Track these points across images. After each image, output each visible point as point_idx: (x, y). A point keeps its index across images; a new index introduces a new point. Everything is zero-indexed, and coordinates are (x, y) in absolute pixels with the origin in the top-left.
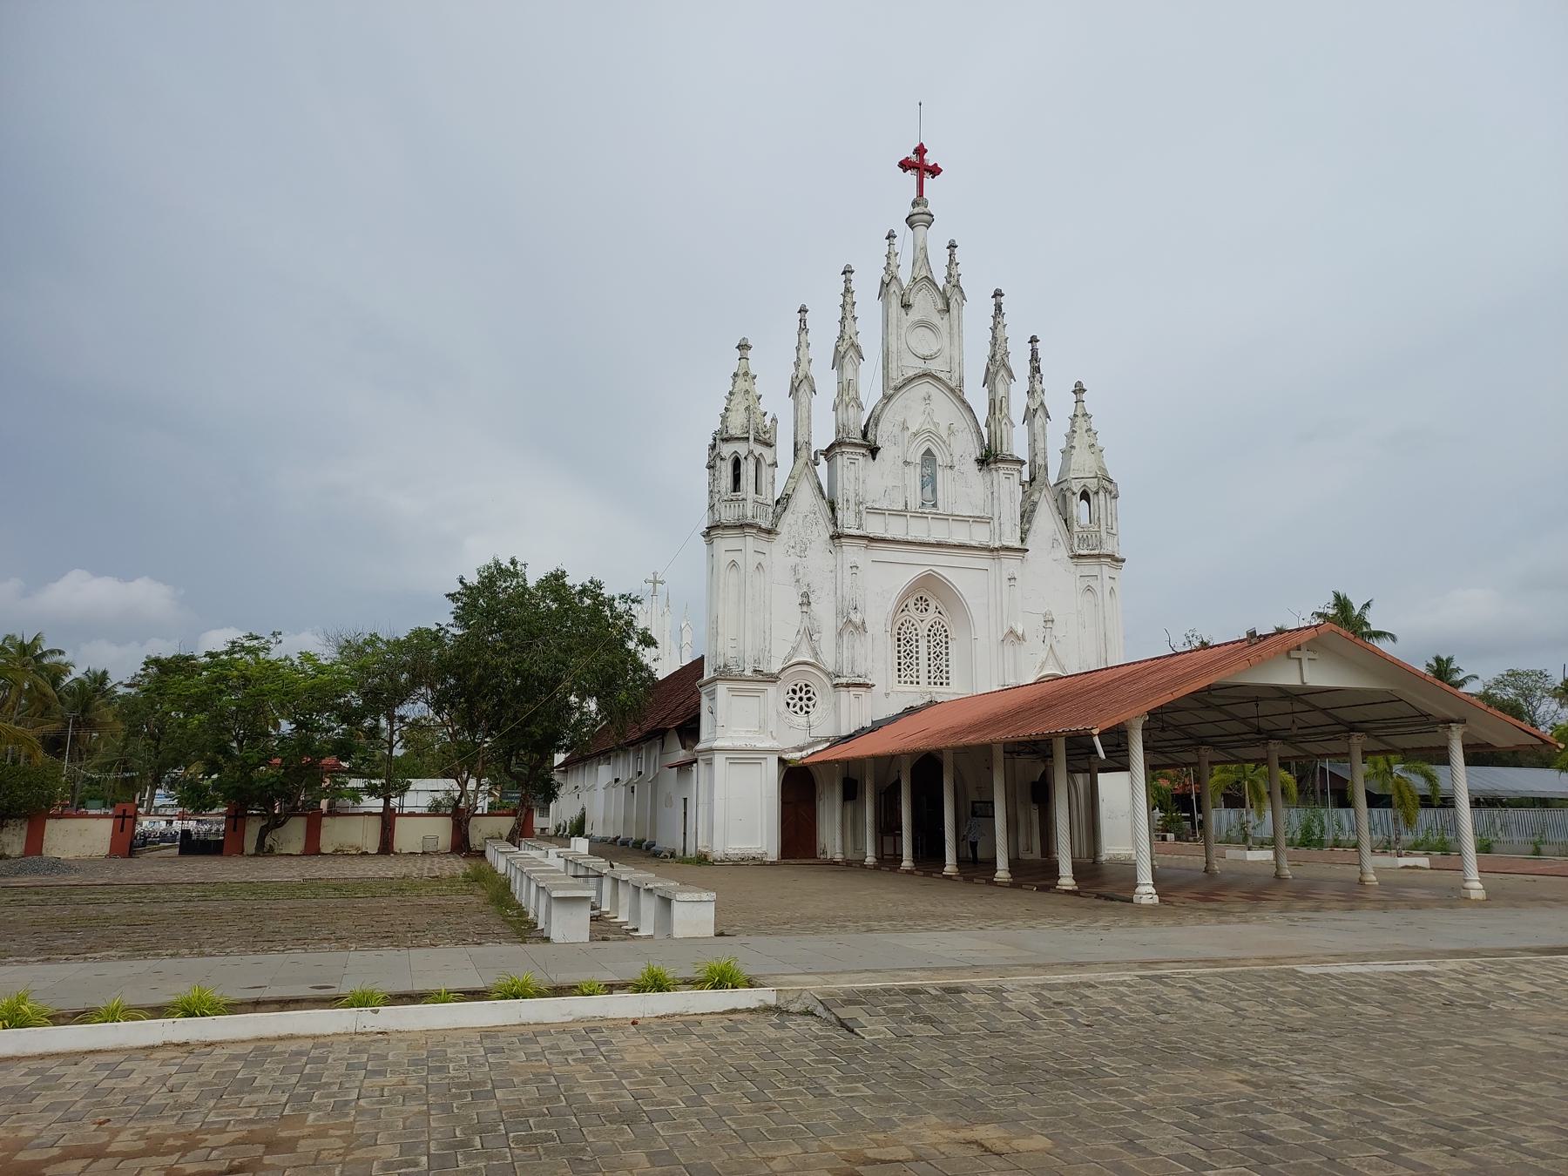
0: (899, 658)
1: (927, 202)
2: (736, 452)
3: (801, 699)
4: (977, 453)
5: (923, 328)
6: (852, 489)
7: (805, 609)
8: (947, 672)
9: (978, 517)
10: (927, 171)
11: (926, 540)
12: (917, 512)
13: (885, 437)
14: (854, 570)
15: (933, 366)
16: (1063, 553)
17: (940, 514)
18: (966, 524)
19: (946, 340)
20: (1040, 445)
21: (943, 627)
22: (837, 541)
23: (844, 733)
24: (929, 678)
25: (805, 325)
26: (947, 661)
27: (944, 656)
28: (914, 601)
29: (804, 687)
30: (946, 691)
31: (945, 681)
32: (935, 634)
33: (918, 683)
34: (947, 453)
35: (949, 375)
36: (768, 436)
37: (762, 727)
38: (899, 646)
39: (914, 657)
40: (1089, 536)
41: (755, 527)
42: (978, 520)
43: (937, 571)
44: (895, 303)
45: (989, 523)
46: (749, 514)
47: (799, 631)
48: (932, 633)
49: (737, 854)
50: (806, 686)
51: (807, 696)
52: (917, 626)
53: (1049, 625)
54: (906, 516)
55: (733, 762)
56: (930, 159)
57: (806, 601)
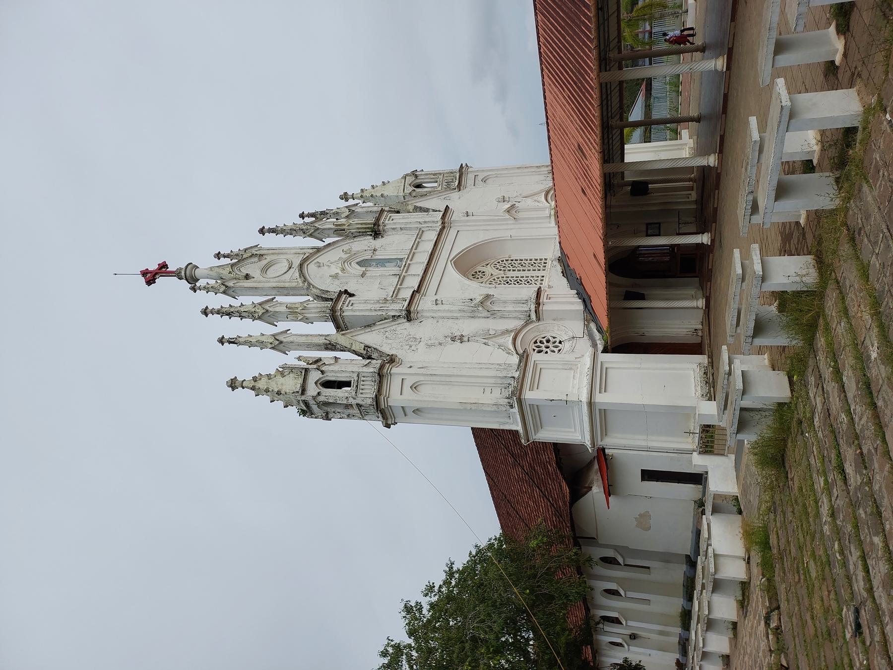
3: (547, 347)
7: (465, 339)
19: (282, 256)
22: (412, 315)
23: (581, 307)
25: (233, 338)
27: (522, 262)
29: (536, 345)
37: (569, 366)
40: (446, 181)
43: (452, 257)
45: (423, 231)
47: (485, 344)
50: (536, 342)
51: (545, 342)
55: (604, 389)
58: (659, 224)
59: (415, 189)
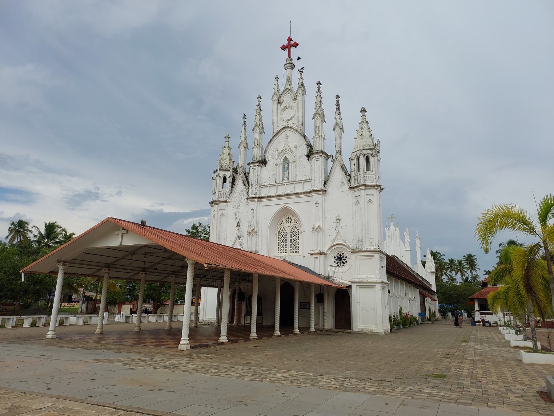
0: (279, 243)
2: (225, 174)
5: (288, 109)
6: (254, 180)
7: (238, 228)
8: (298, 247)
9: (305, 180)
10: (292, 46)
11: (283, 194)
12: (280, 183)
13: (270, 156)
15: (289, 124)
16: (347, 187)
17: (290, 182)
18: (301, 184)
20: (338, 142)
26: (299, 242)
27: (297, 240)
28: (285, 219)
30: (299, 255)
31: (297, 251)
32: (294, 232)
33: (279, 253)
34: (293, 157)
35: (296, 124)
36: (229, 167)
38: (279, 238)
39: (285, 242)
41: (218, 201)
42: (306, 181)
44: (276, 102)
46: (217, 197)
48: (297, 231)
49: (207, 321)
52: (286, 229)
53: (338, 221)
54: (276, 185)
56: (292, 42)
57: (238, 225)
59: (366, 156)
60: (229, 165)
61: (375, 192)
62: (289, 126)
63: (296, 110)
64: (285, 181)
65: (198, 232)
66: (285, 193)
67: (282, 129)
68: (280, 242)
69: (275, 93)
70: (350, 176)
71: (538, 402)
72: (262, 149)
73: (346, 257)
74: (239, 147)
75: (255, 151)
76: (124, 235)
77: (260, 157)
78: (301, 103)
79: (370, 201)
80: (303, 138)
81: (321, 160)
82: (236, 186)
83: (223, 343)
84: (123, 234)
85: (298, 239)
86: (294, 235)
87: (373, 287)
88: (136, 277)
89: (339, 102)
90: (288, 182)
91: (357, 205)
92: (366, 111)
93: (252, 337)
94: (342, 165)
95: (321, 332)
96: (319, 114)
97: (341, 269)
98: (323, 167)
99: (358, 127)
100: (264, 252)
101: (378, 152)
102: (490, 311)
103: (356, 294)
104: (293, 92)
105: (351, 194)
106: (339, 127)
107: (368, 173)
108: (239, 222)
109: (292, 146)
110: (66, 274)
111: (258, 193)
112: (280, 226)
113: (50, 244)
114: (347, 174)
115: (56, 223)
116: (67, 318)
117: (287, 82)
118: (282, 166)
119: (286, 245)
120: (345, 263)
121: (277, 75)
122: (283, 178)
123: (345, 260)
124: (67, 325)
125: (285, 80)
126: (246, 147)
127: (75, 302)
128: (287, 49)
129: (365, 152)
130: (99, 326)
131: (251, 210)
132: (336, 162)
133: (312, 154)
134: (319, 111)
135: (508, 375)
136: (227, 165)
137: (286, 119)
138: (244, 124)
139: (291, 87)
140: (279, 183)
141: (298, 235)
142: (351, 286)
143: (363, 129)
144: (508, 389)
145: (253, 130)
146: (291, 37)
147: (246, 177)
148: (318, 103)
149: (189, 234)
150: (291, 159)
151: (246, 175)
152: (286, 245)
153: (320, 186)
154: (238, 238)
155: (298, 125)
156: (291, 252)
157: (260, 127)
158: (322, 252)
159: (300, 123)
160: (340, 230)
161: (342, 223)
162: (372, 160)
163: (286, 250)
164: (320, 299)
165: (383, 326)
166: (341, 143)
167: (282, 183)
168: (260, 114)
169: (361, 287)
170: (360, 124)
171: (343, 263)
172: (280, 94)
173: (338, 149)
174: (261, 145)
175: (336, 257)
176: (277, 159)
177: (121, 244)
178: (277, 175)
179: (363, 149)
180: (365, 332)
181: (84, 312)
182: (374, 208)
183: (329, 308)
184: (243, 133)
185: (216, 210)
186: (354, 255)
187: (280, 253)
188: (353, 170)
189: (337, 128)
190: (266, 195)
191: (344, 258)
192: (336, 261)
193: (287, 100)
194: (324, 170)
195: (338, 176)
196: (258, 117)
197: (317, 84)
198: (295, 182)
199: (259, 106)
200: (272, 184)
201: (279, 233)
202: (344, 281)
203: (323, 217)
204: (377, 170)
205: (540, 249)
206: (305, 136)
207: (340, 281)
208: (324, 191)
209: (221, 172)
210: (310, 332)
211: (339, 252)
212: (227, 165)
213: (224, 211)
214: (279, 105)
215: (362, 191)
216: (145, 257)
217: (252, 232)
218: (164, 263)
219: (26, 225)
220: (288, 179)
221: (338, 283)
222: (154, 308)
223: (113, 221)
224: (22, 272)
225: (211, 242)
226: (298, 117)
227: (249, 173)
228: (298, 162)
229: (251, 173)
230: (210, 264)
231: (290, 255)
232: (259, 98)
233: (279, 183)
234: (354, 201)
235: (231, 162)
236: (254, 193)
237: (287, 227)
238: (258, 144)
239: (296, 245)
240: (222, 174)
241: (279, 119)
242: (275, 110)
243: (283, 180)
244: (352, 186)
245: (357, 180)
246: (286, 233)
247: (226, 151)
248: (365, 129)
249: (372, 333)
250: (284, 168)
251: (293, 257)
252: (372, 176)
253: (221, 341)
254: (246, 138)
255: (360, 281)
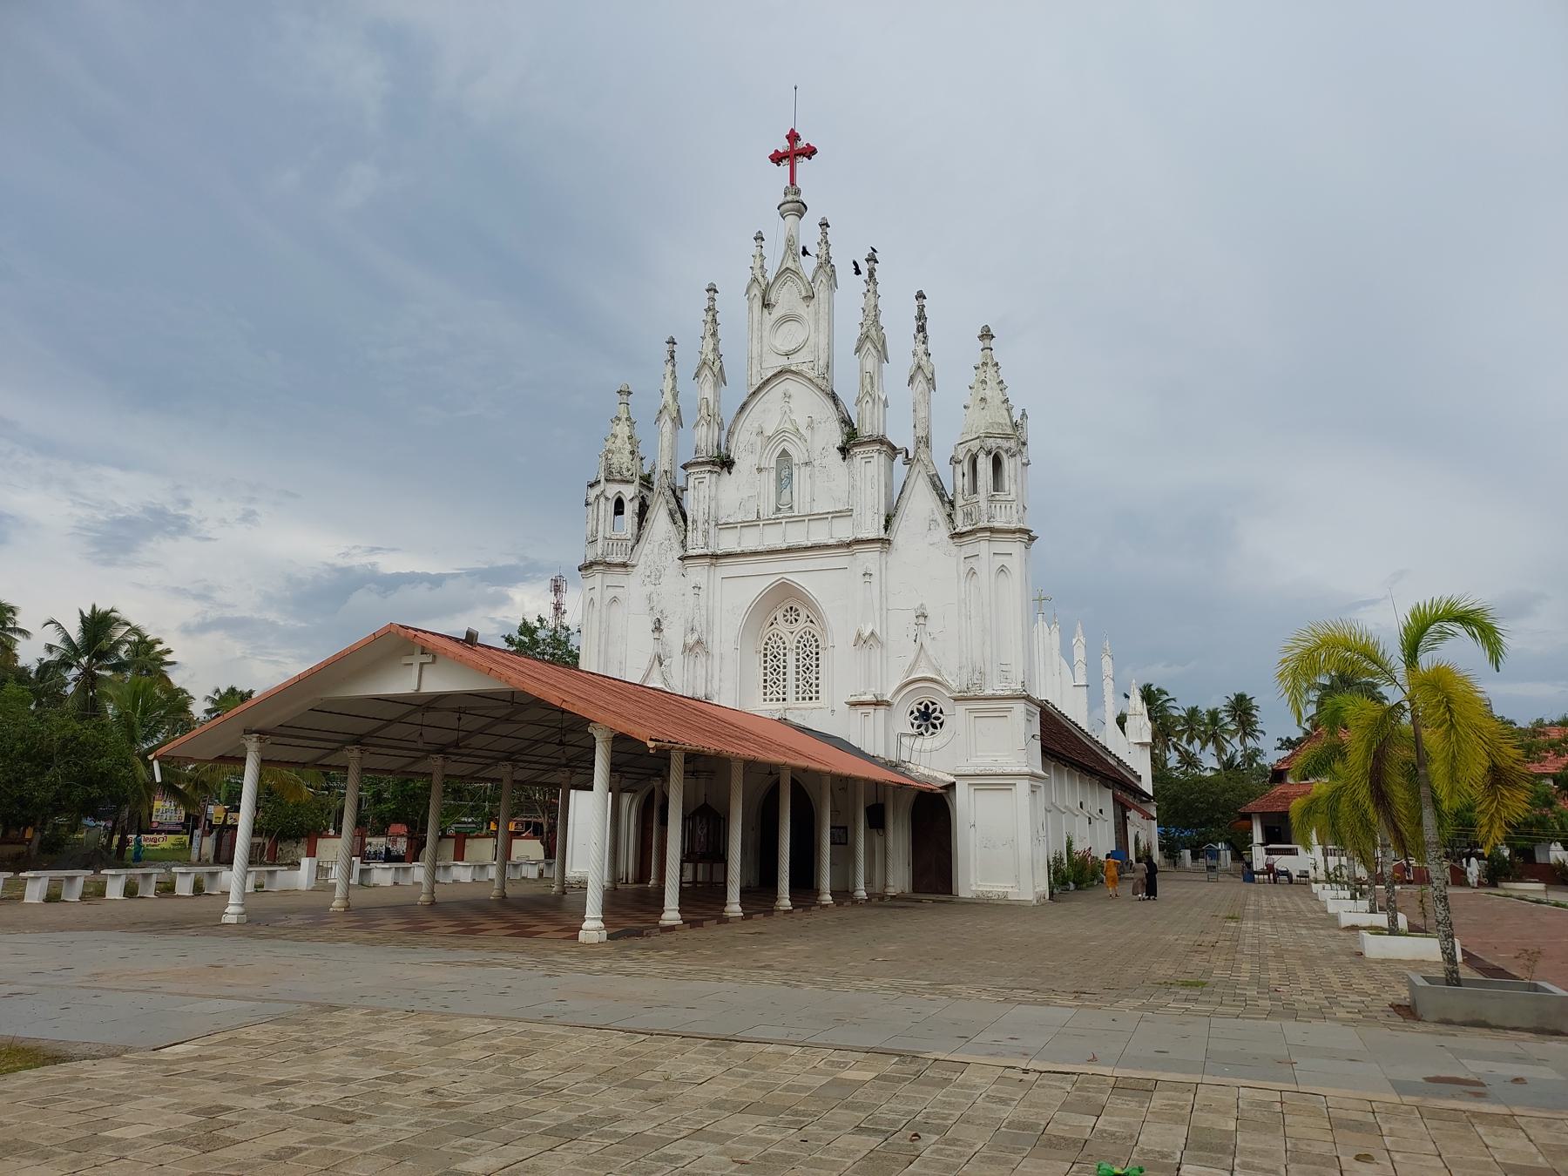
0: (765, 675)
1: (799, 190)
2: (620, 492)
4: (838, 439)
5: (789, 323)
8: (817, 686)
10: (800, 155)
11: (778, 547)
14: (696, 590)
15: (794, 362)
16: (943, 531)
20: (922, 414)
21: (813, 636)
24: (798, 693)
26: (817, 673)
30: (819, 705)
31: (814, 695)
32: (805, 646)
33: (765, 700)
34: (805, 451)
38: (765, 662)
39: (781, 673)
41: (602, 564)
42: (838, 515)
44: (758, 303)
46: (600, 552)
48: (814, 644)
52: (785, 638)
53: (921, 620)
56: (801, 145)
57: (658, 628)
58: (846, 844)
60: (630, 467)
61: (1016, 548)
62: (793, 368)
63: (812, 327)
64: (783, 513)
65: (535, 643)
66: (784, 546)
67: (775, 376)
68: (769, 673)
69: (755, 280)
70: (952, 503)
71: (1389, 1019)
72: (721, 428)
73: (941, 712)
74: (658, 419)
75: (702, 431)
76: (425, 666)
77: (715, 448)
78: (824, 308)
79: (1002, 569)
80: (832, 403)
81: (879, 460)
82: (651, 523)
83: (672, 928)
84: (422, 664)
85: (817, 666)
86: (804, 656)
87: (1008, 788)
88: (420, 767)
89: (925, 309)
90: (791, 517)
91: (968, 581)
92: (993, 337)
93: (730, 914)
94: (933, 475)
95: (879, 900)
96: (872, 340)
97: (928, 742)
98: (882, 478)
99: (972, 377)
100: (726, 697)
101: (1024, 444)
102: (1291, 844)
103: (966, 806)
104: (805, 279)
105: (954, 549)
106: (923, 375)
107: (997, 498)
108: (659, 620)
109: (802, 423)
110: (264, 762)
111: (711, 543)
112: (768, 632)
113: (97, 672)
114: (946, 499)
115: (112, 611)
116: (213, 875)
117: (785, 253)
118: (773, 474)
119: (784, 680)
120: (939, 726)
121: (760, 232)
122: (777, 507)
123: (937, 718)
124: (215, 893)
125: (783, 247)
126: (678, 421)
127: (159, 832)
128: (785, 162)
129: (991, 443)
130: (339, 893)
131: (694, 588)
132: (918, 468)
133: (855, 445)
134: (873, 332)
135: (1335, 980)
136: (624, 466)
137: (785, 349)
138: (669, 358)
139: (798, 264)
140: (767, 520)
141: (817, 654)
142: (954, 784)
143: (986, 383)
144: (1333, 1002)
145: (697, 375)
146: (796, 131)
147: (678, 501)
148: (869, 312)
149: (512, 649)
150: (797, 455)
151: (677, 495)
152: (784, 680)
153: (874, 529)
154: (657, 662)
155: (816, 366)
156: (797, 699)
157: (716, 369)
158: (879, 699)
159: (822, 363)
160: (927, 643)
161: (933, 625)
162: (1008, 465)
163: (784, 693)
164: (876, 819)
165: (1033, 884)
166: (928, 419)
167: (774, 519)
168: (714, 334)
169: (979, 788)
170: (979, 371)
171: (934, 726)
172: (768, 283)
173: (921, 433)
174: (716, 417)
175: (915, 711)
176: (761, 456)
177: (418, 690)
178: (762, 496)
179: (987, 437)
180: (989, 899)
181: (207, 860)
182: (1013, 593)
183: (898, 840)
184: (669, 382)
185: (598, 588)
186: (961, 708)
187: (768, 702)
188: (959, 490)
189: (920, 377)
190: (733, 550)
191: (937, 714)
192: (916, 723)
193: (787, 296)
194: (886, 487)
195: (921, 504)
196: (710, 341)
197: (867, 260)
198: (810, 518)
199: (710, 313)
200: (744, 522)
201: (766, 649)
202: (936, 774)
203: (881, 609)
204: (1020, 491)
205: (1402, 714)
206: (834, 397)
207: (926, 772)
208: (885, 542)
209: (610, 485)
210: (856, 902)
211: (922, 700)
212: (624, 466)
213: (618, 590)
214: (766, 311)
215: (984, 545)
216: (459, 719)
217: (696, 647)
218: (494, 730)
219: (10, 615)
220: (791, 507)
221: (922, 778)
222: (409, 846)
223: (402, 634)
224: (153, 759)
225: (582, 671)
226: (817, 345)
227: (684, 490)
228: (816, 463)
229: (691, 491)
230: (659, 741)
231: (793, 706)
232: (710, 290)
233: (767, 520)
234: (963, 568)
235: (637, 460)
236: (701, 544)
237: (788, 633)
238: (711, 413)
239: (811, 681)
240: (612, 490)
241: (765, 349)
242: (756, 326)
243: (778, 510)
244: (957, 530)
245: (971, 515)
246: (785, 649)
247: (622, 430)
248: (992, 383)
249: (1007, 902)
250: (779, 479)
251: (803, 712)
252: (1008, 506)
253: (667, 923)
254: (675, 396)
255: (978, 772)
